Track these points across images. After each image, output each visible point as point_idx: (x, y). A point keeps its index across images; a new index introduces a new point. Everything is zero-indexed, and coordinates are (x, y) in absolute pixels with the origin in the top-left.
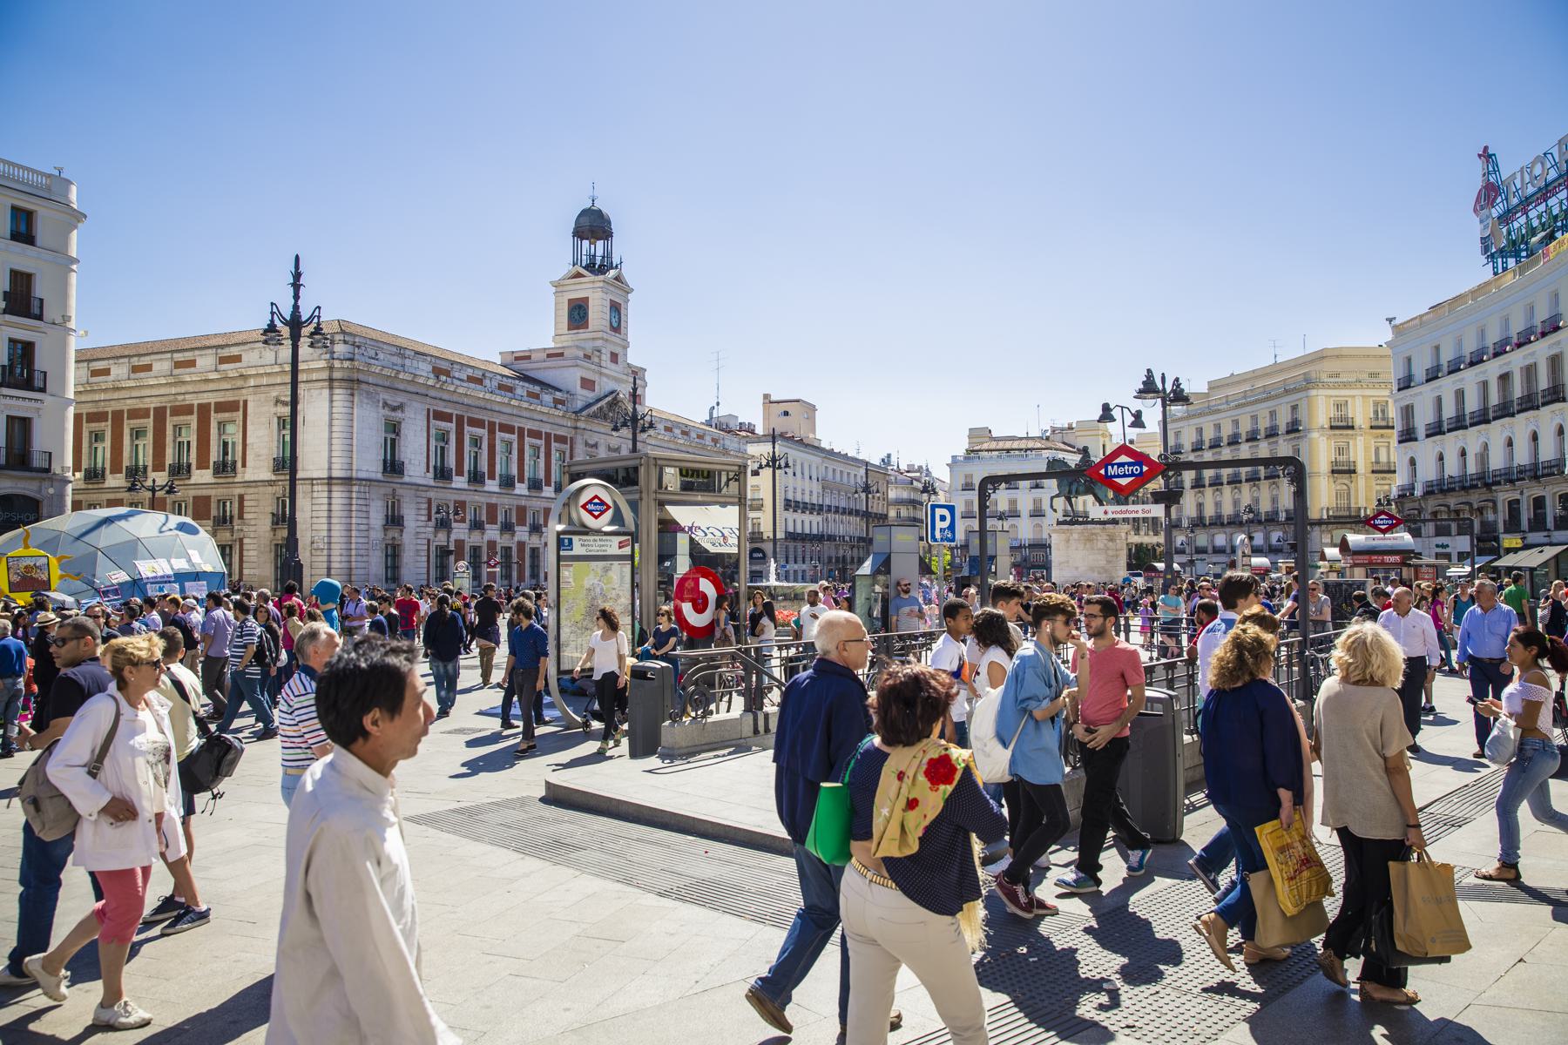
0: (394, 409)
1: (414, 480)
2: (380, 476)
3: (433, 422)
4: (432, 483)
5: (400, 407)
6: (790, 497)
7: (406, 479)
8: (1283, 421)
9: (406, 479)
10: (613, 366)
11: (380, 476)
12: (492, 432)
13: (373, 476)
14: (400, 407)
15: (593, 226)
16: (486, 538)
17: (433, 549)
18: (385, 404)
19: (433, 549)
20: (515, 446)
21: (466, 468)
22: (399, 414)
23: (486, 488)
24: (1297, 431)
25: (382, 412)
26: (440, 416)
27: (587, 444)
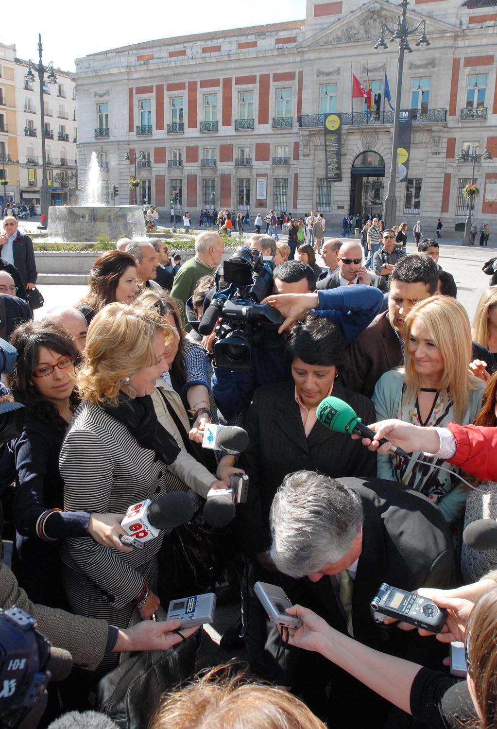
0: (101, 96)
2: (93, 140)
3: (136, 97)
4: (136, 138)
5: (107, 93)
7: (112, 139)
9: (112, 139)
11: (93, 140)
13: (89, 141)
14: (107, 93)
16: (185, 174)
18: (96, 94)
20: (220, 96)
22: (106, 98)
23: (186, 135)
25: (94, 99)
27: (320, 73)
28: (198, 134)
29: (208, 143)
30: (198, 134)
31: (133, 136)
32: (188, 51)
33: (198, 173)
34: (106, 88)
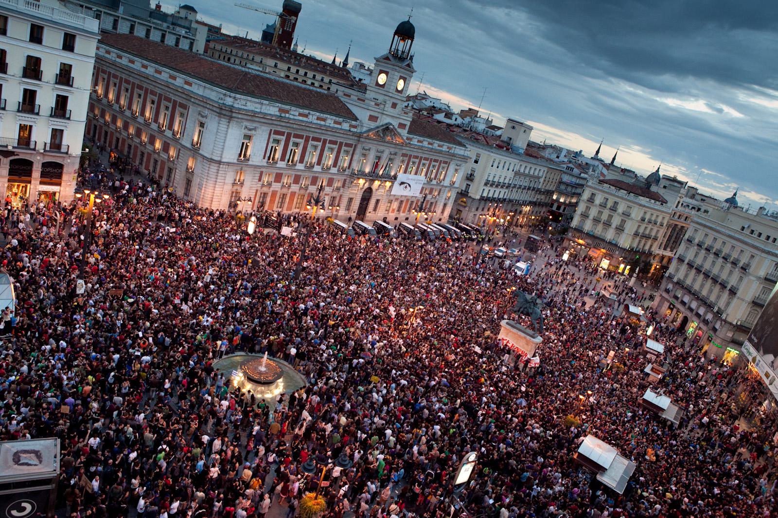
0: (250, 130)
1: (254, 163)
2: (235, 161)
5: (255, 129)
6: (491, 179)
7: (250, 163)
8: (743, 260)
10: (392, 110)
11: (235, 161)
12: (307, 141)
13: (232, 161)
15: (406, 31)
16: (290, 191)
17: (259, 194)
19: (259, 194)
21: (287, 157)
22: (253, 132)
24: (745, 270)
26: (277, 133)
27: (364, 149)
28: (303, 168)
29: (307, 174)
30: (303, 168)
31: (264, 163)
32: (310, 117)
33: (297, 191)
34: (255, 125)
